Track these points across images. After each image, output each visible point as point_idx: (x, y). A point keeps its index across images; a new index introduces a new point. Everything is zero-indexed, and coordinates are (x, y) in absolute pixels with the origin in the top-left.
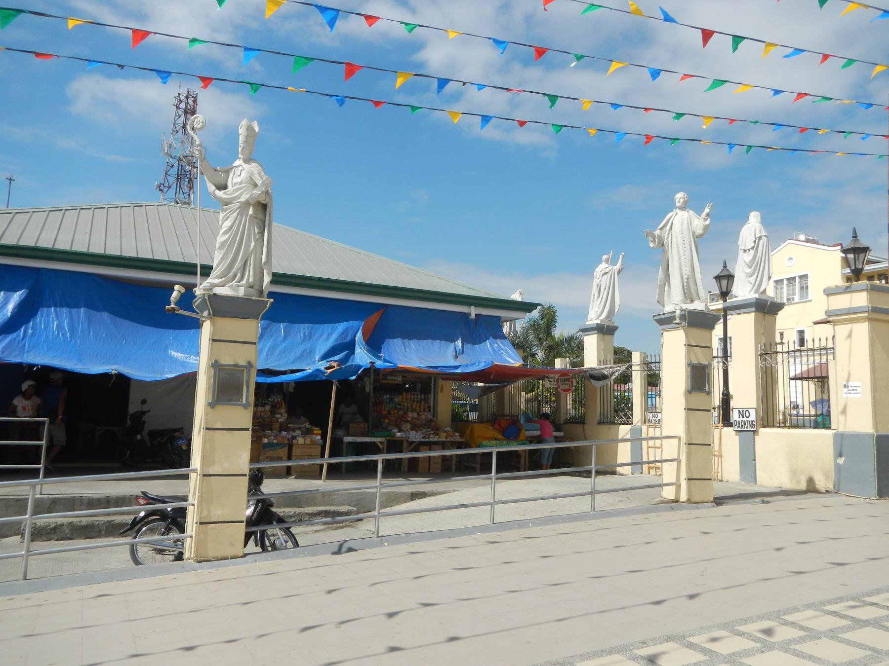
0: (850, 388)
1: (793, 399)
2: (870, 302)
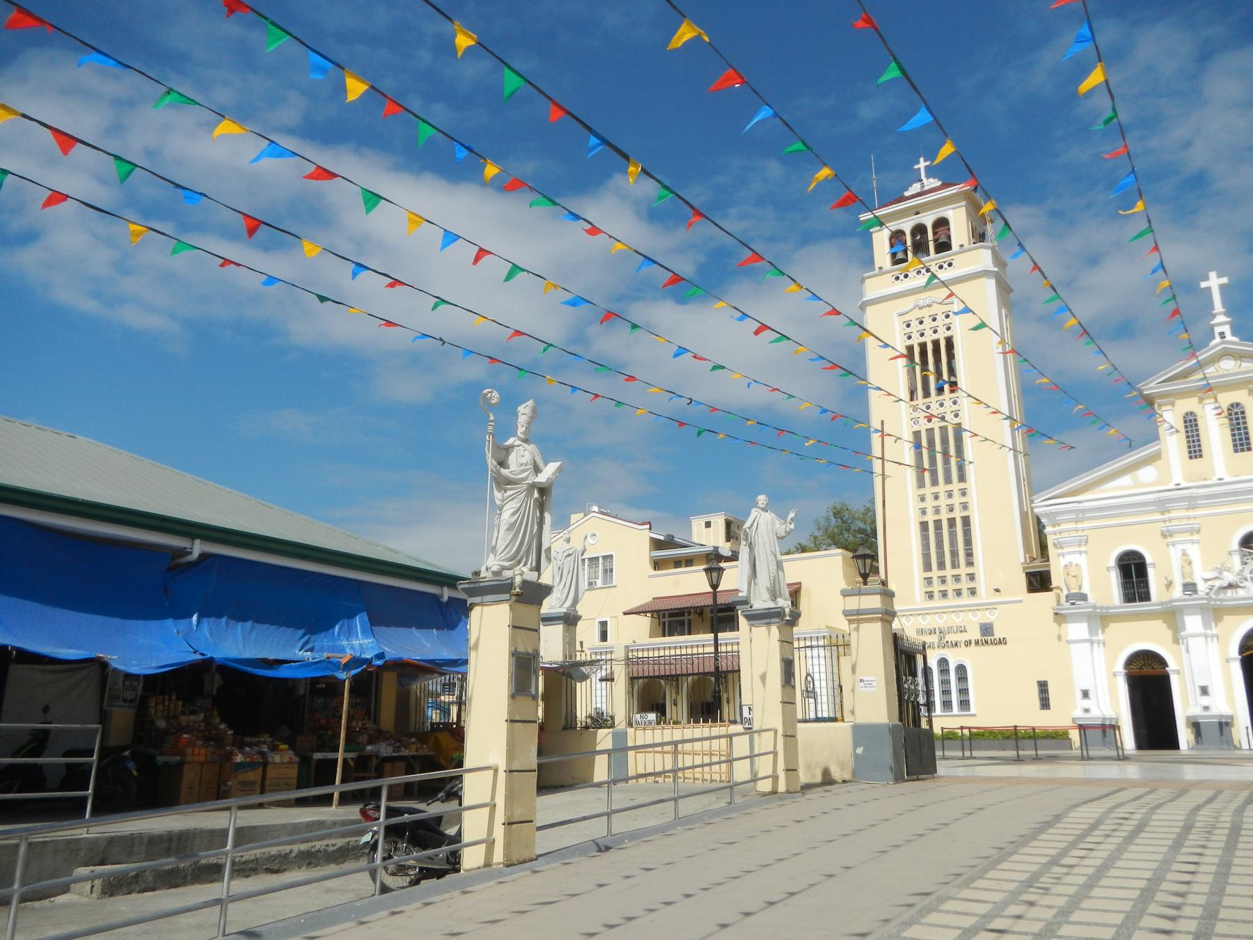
0: (865, 682)
1: (599, 706)
2: (883, 605)
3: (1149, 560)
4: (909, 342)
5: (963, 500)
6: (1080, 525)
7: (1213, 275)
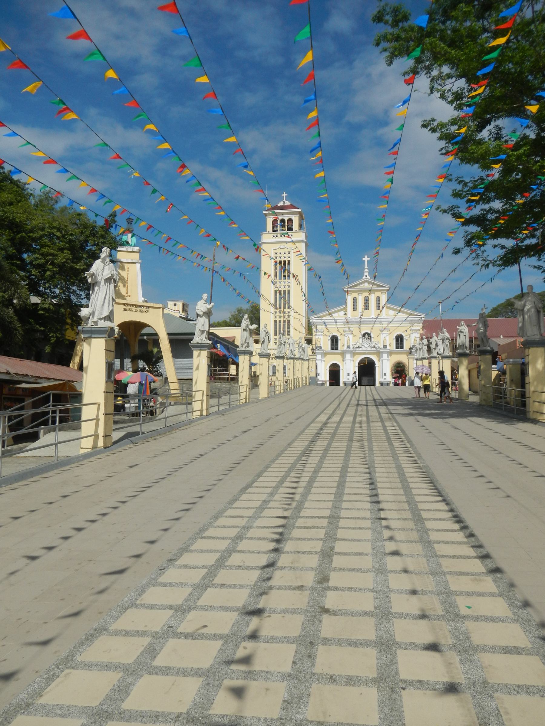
7: (366, 256)
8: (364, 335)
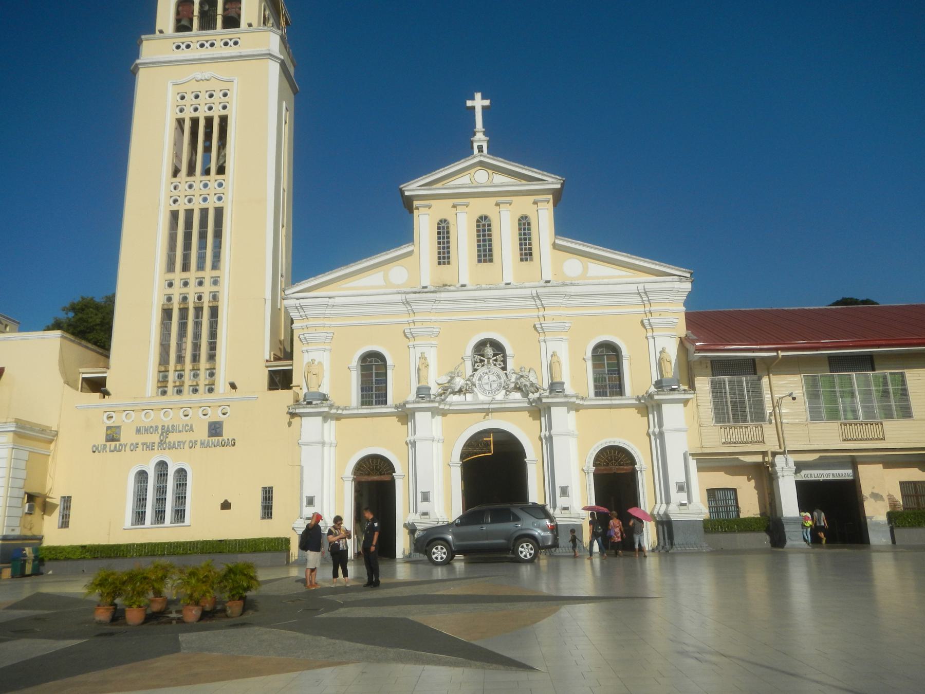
3: (389, 362)
4: (181, 115)
5: (214, 289)
6: (327, 322)
7: (478, 96)
8: (480, 347)
